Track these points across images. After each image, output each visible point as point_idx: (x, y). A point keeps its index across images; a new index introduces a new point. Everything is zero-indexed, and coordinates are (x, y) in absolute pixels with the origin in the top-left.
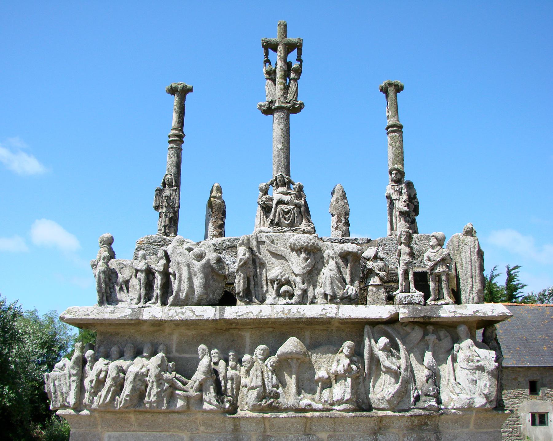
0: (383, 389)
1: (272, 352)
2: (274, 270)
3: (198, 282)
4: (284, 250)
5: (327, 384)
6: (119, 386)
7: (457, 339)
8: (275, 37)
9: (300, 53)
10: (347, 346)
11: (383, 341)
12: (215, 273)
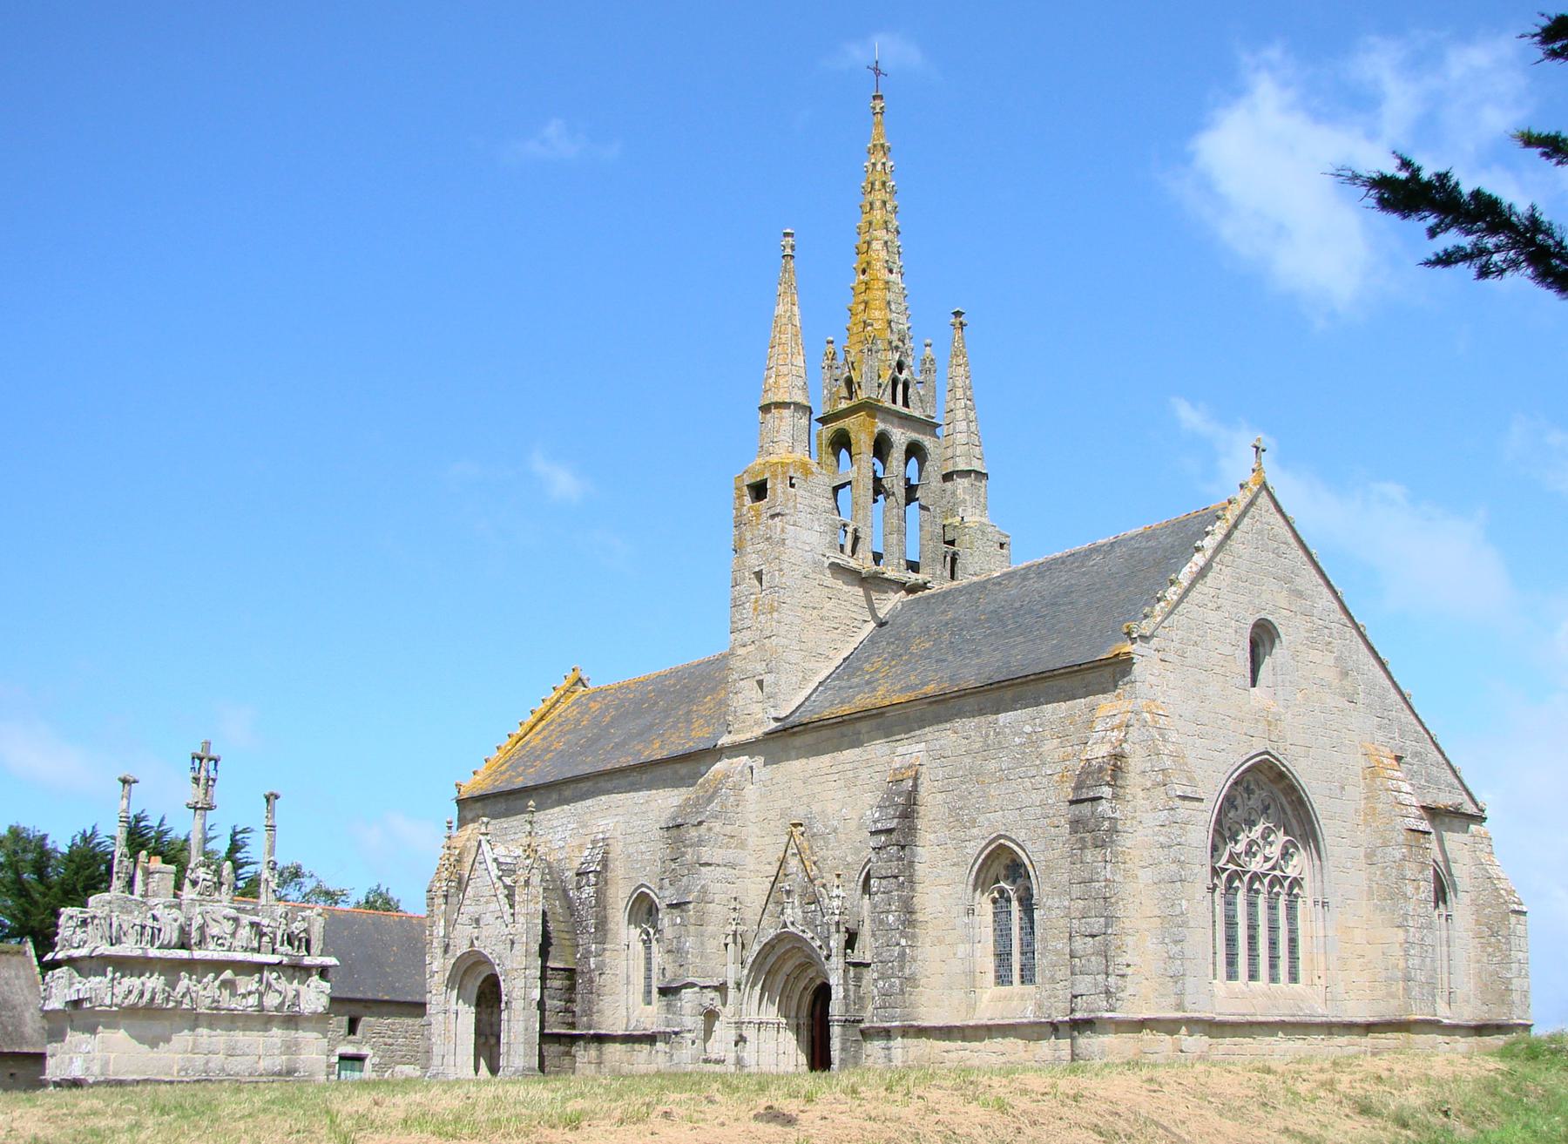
0: (271, 1000)
1: (216, 978)
2: (214, 930)
3: (175, 935)
4: (220, 919)
5: (244, 996)
6: (142, 995)
7: (310, 976)
8: (199, 752)
10: (257, 976)
11: (275, 975)
12: (184, 932)
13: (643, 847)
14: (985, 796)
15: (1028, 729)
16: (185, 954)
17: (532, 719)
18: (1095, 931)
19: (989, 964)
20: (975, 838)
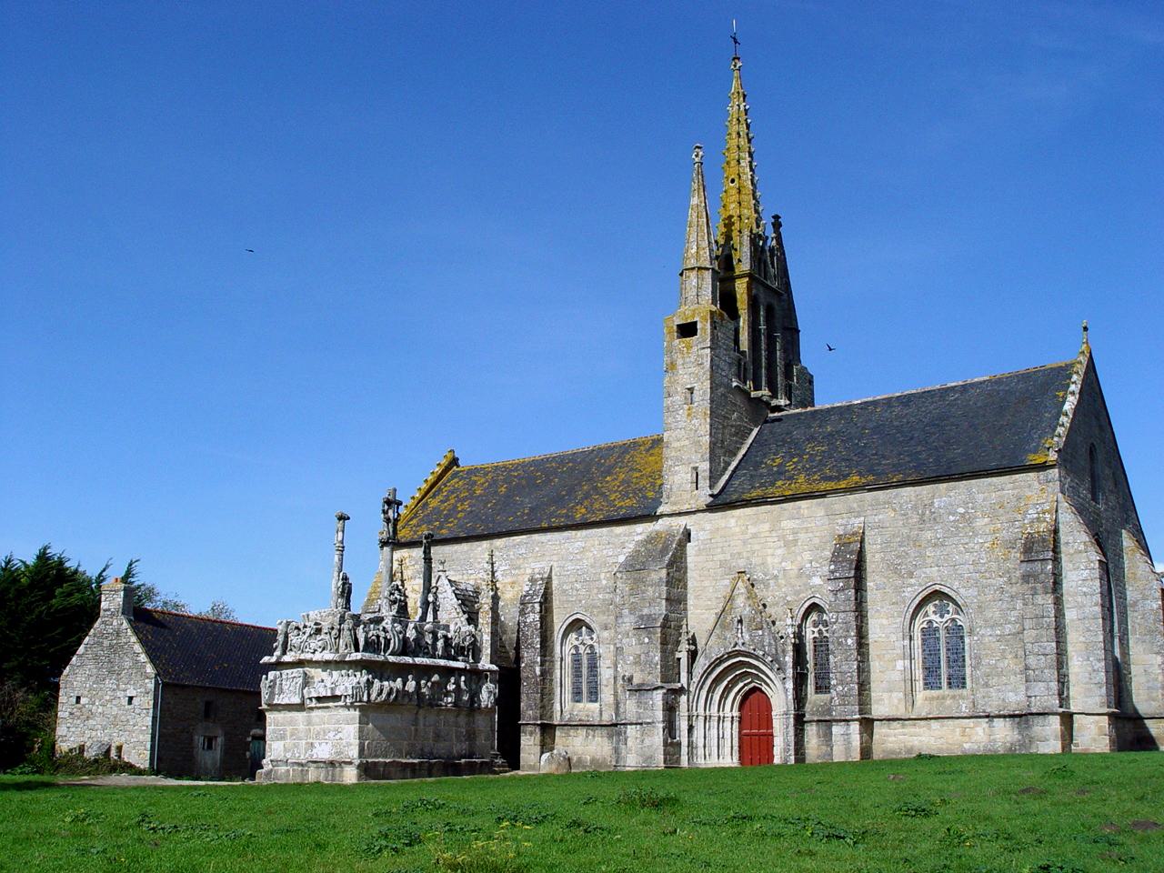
9: (398, 508)
13: (578, 586)
14: (922, 556)
15: (961, 510)
16: (409, 660)
17: (425, 486)
18: (1047, 652)
19: (919, 674)
20: (912, 585)
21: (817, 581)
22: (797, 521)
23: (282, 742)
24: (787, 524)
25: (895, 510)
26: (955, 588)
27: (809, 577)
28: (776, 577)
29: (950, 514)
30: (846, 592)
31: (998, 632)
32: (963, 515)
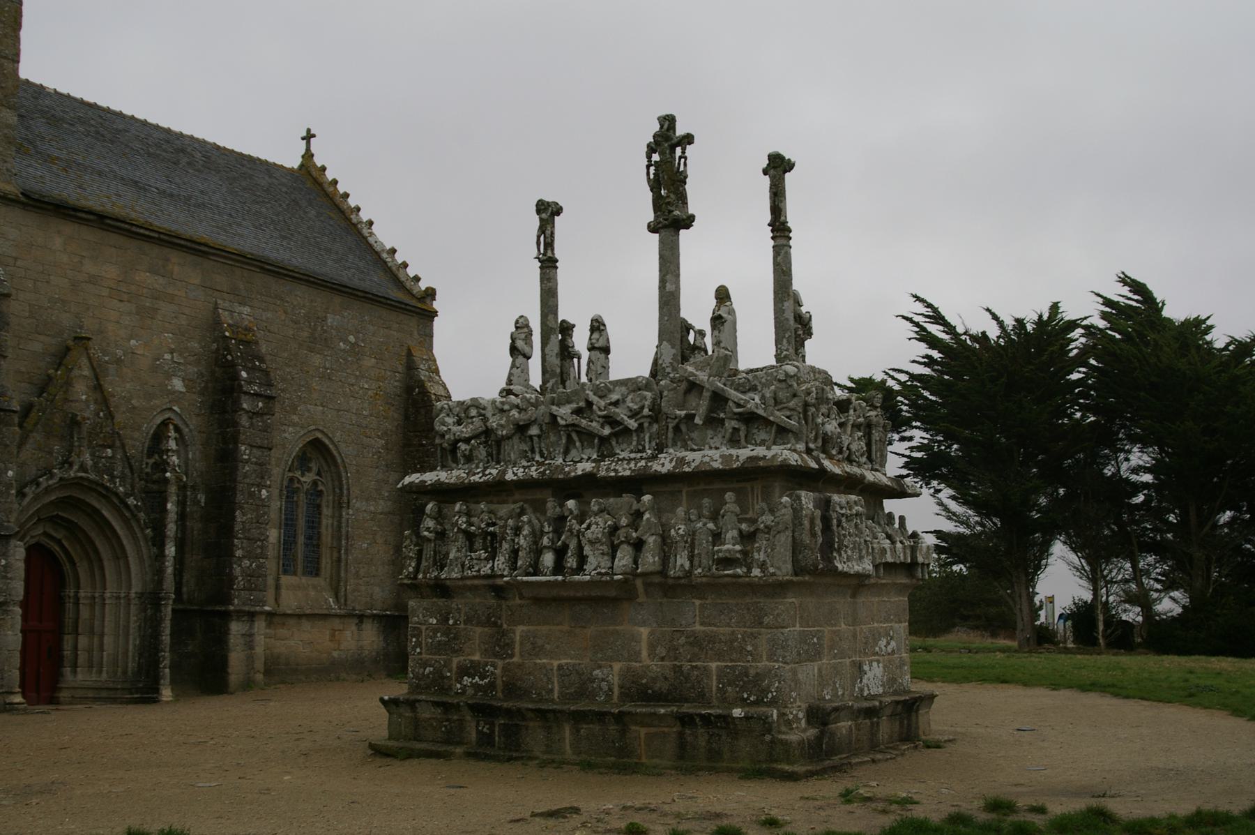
15: (352, 339)
21: (178, 384)
22: (161, 280)
23: (816, 665)
24: (144, 277)
25: (285, 312)
26: (336, 439)
27: (169, 376)
28: (119, 361)
29: (341, 340)
30: (265, 417)
31: (372, 508)
32: (353, 345)
